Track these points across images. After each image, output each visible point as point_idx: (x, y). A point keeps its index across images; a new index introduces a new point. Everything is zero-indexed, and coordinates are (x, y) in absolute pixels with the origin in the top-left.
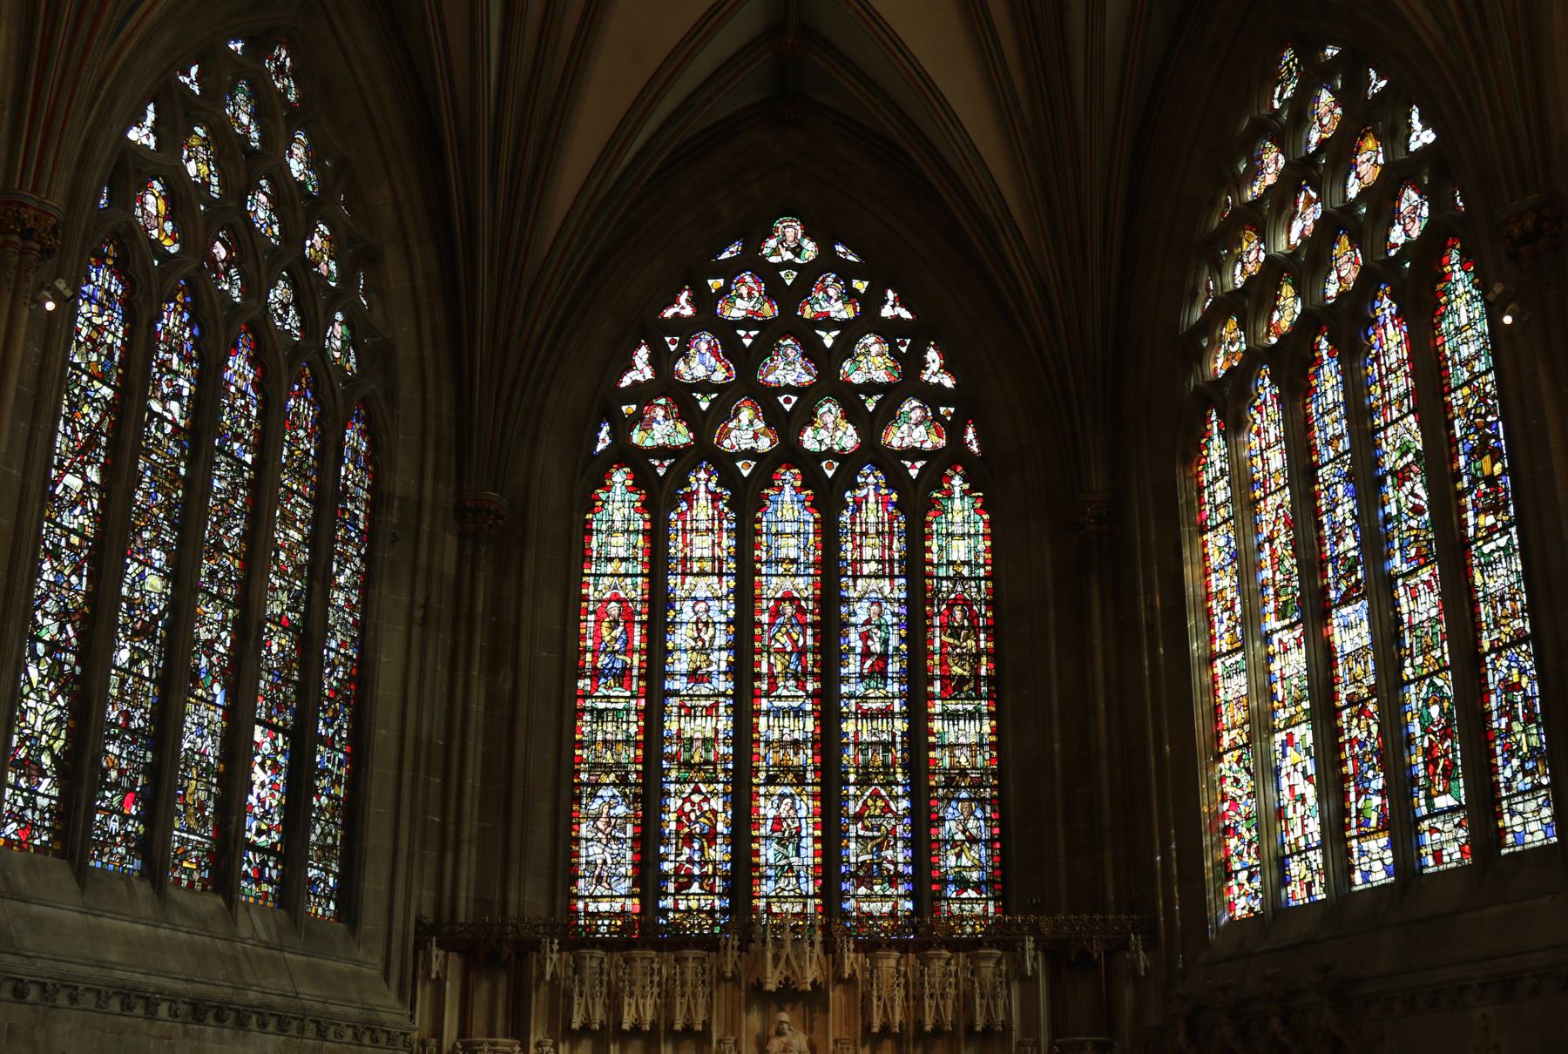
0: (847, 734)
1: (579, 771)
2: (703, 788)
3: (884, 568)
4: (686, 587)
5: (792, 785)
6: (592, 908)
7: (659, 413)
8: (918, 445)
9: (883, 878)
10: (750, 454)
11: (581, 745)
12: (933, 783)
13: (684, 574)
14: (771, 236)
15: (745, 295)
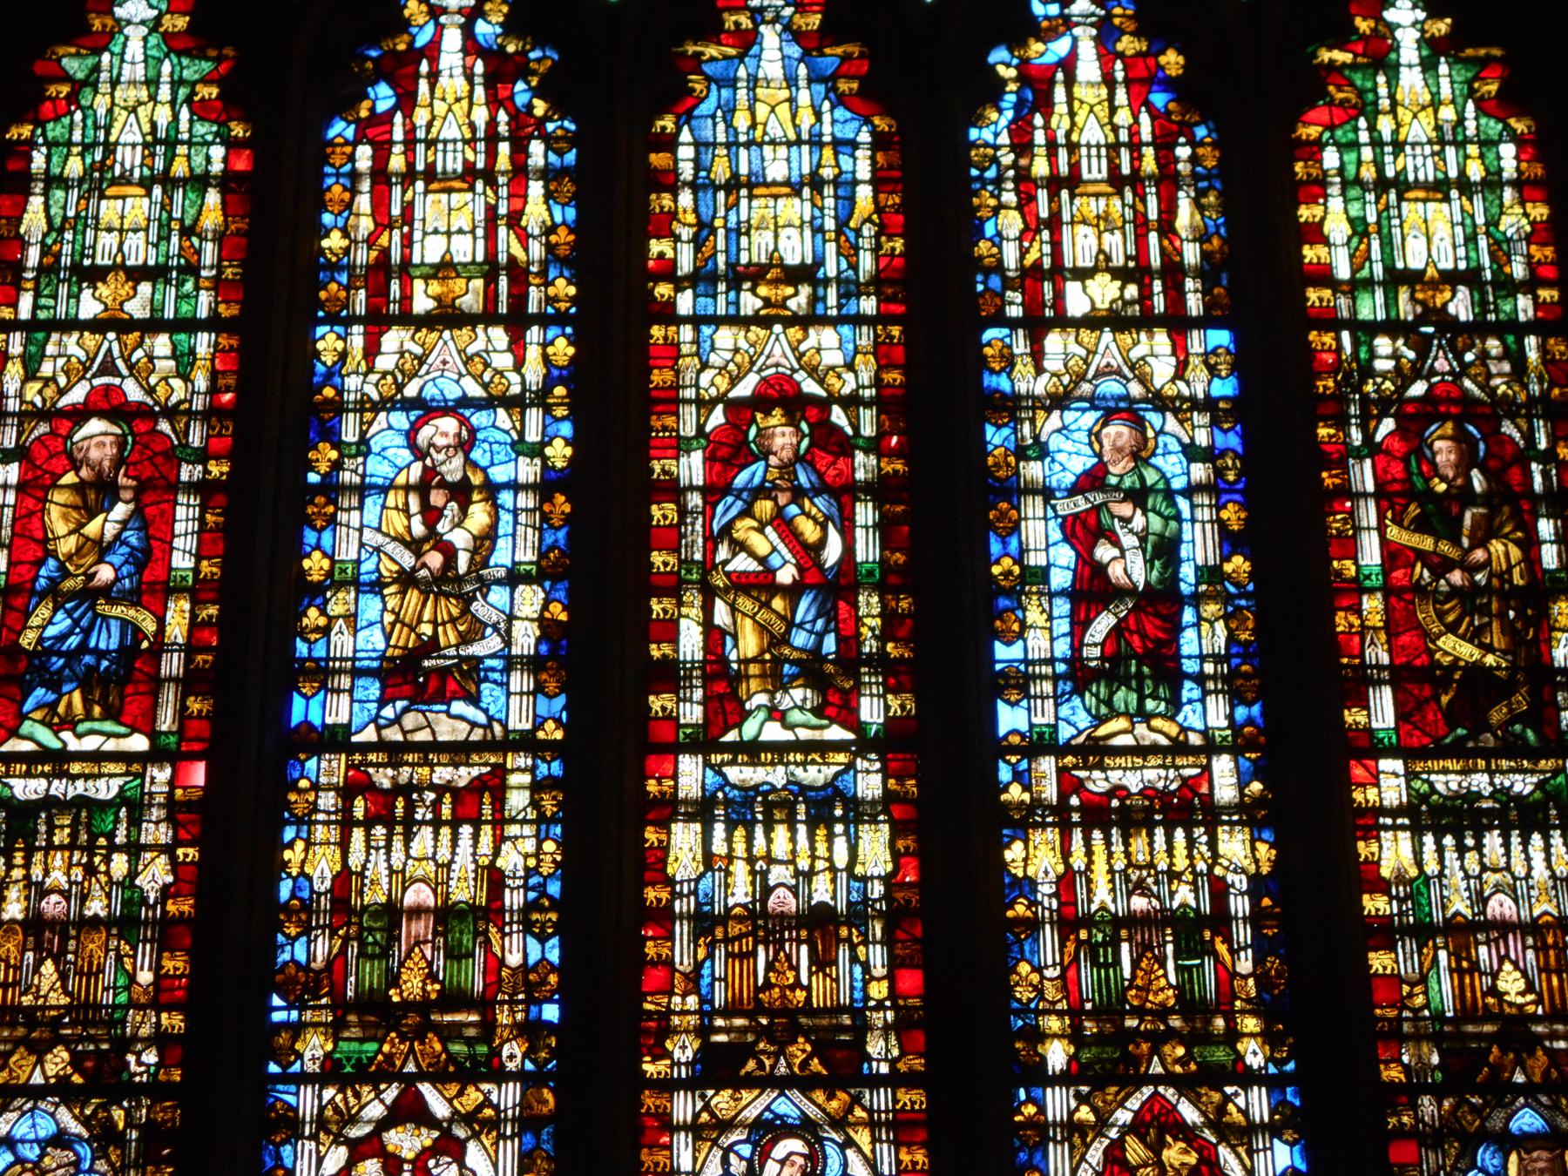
0: (1027, 886)
2: (437, 1103)
3: (1145, 296)
4: (384, 362)
5: (805, 1083)
12: (1393, 1074)
13: (377, 322)
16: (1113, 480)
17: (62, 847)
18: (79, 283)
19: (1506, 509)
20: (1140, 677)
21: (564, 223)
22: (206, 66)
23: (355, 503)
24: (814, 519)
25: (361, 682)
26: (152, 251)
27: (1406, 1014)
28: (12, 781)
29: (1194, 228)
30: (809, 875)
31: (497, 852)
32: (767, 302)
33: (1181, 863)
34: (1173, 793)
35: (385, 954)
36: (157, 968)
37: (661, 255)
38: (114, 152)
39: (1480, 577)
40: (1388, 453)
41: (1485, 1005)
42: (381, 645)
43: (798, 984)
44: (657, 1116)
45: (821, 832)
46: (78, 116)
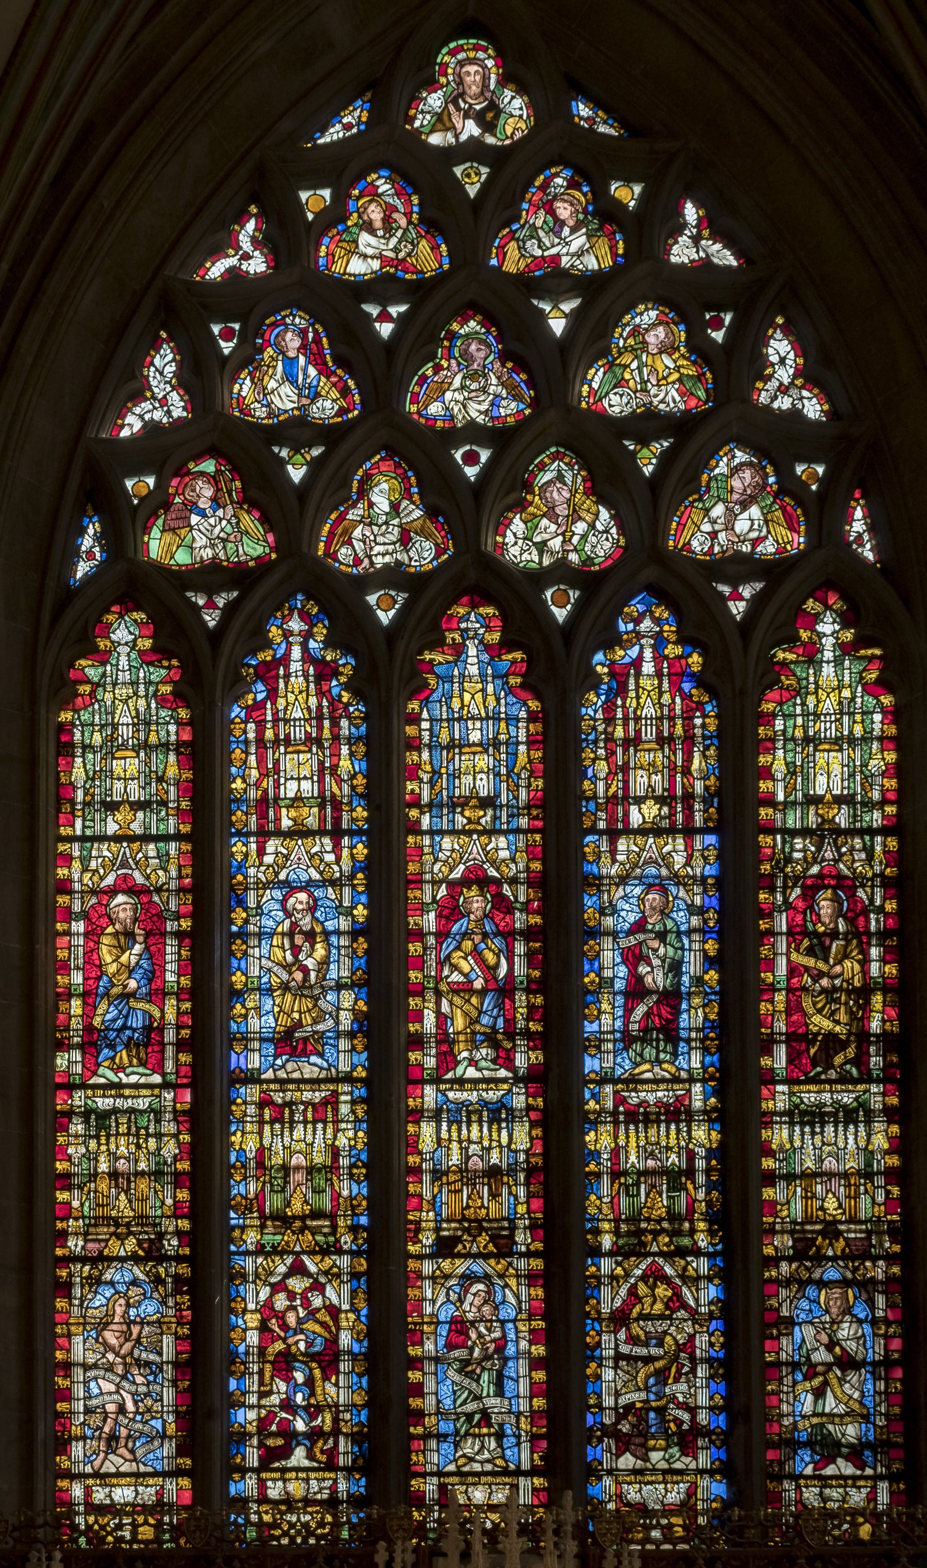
3: (672, 814)
4: (269, 859)
5: (486, 1257)
6: (99, 1495)
8: (746, 548)
9: (668, 1437)
11: (65, 1181)
12: (769, 1251)
13: (263, 834)
14: (432, 85)
15: (378, 224)
16: (650, 927)
17: (123, 1135)
18: (106, 811)
19: (855, 942)
20: (658, 1040)
21: (360, 772)
22: (164, 672)
23: (256, 943)
24: (493, 951)
27: (778, 1220)
28: (97, 1100)
30: (489, 1149)
31: (335, 1137)
32: (470, 821)
33: (673, 1142)
34: (670, 1105)
35: (283, 1190)
36: (174, 1197)
37: (413, 790)
38: (117, 729)
39: (837, 982)
40: (795, 909)
41: (817, 1216)
42: (273, 1025)
43: (483, 1206)
44: (415, 1272)
45: (495, 1127)
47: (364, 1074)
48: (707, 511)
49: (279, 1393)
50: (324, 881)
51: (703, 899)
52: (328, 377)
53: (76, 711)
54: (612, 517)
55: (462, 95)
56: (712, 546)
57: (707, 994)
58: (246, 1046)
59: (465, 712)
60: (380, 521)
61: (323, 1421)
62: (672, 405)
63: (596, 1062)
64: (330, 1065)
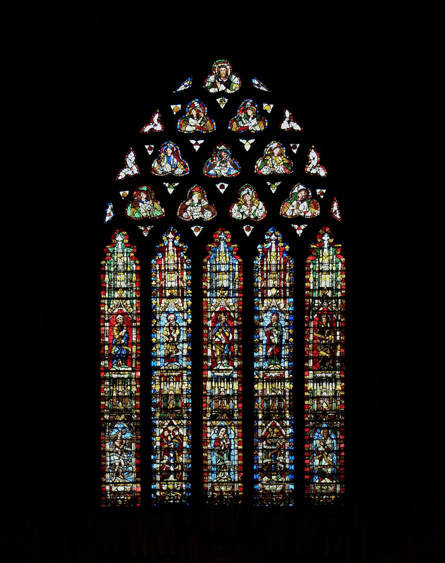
0: (258, 391)
1: (103, 414)
2: (175, 423)
3: (280, 292)
4: (163, 305)
5: (225, 420)
6: (114, 489)
7: (144, 196)
8: (302, 214)
10: (200, 222)
12: (307, 419)
13: (161, 297)
14: (211, 74)
15: (195, 116)
16: (273, 325)
17: (120, 385)
20: (275, 358)
21: (189, 279)
22: (132, 249)
25: (161, 359)
26: (125, 285)
29: (288, 280)
30: (227, 389)
31: (182, 386)
33: (279, 388)
34: (279, 377)
35: (167, 401)
36: (135, 403)
37: (205, 285)
40: (315, 320)
43: (224, 406)
45: (228, 383)
46: (112, 259)
47: (190, 368)
48: (291, 203)
49: (166, 459)
50: (179, 311)
51: (289, 317)
52: (180, 162)
53: (106, 261)
54: (263, 205)
55: (220, 77)
56: (293, 214)
57: (290, 345)
58: (156, 360)
59: (220, 262)
60: (195, 206)
61: (178, 467)
62: (281, 172)
63: (258, 364)
64: (180, 365)
